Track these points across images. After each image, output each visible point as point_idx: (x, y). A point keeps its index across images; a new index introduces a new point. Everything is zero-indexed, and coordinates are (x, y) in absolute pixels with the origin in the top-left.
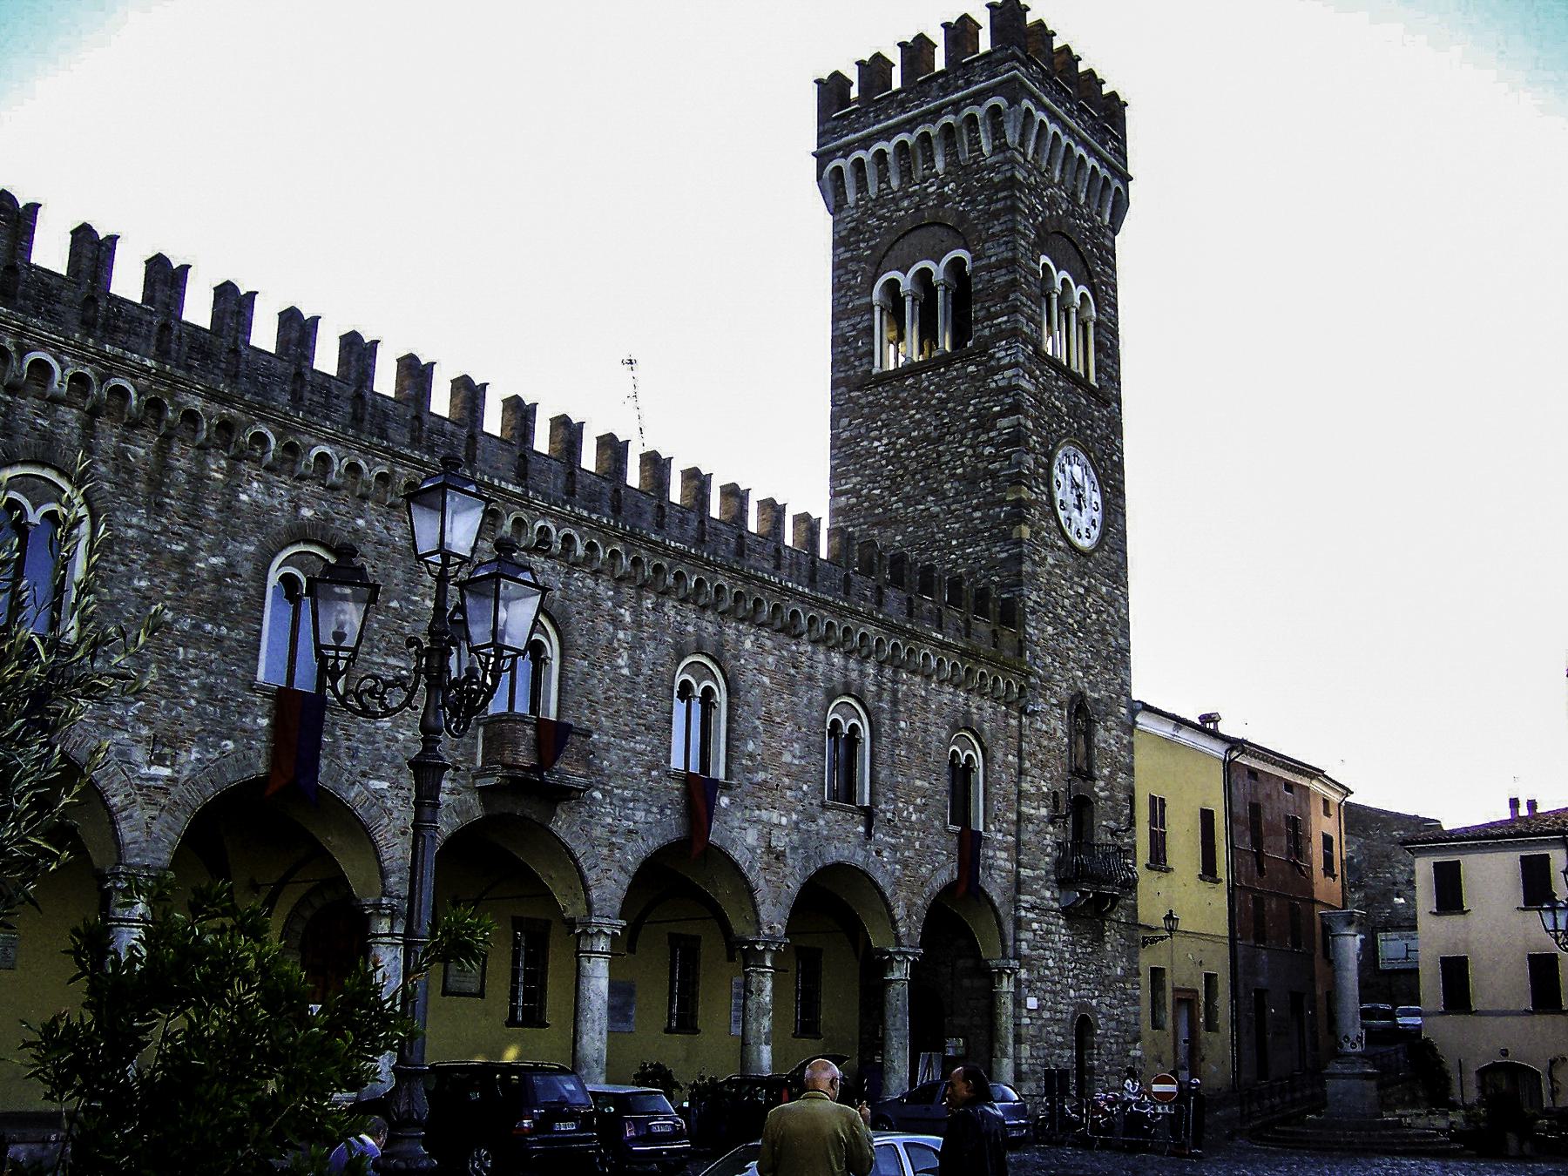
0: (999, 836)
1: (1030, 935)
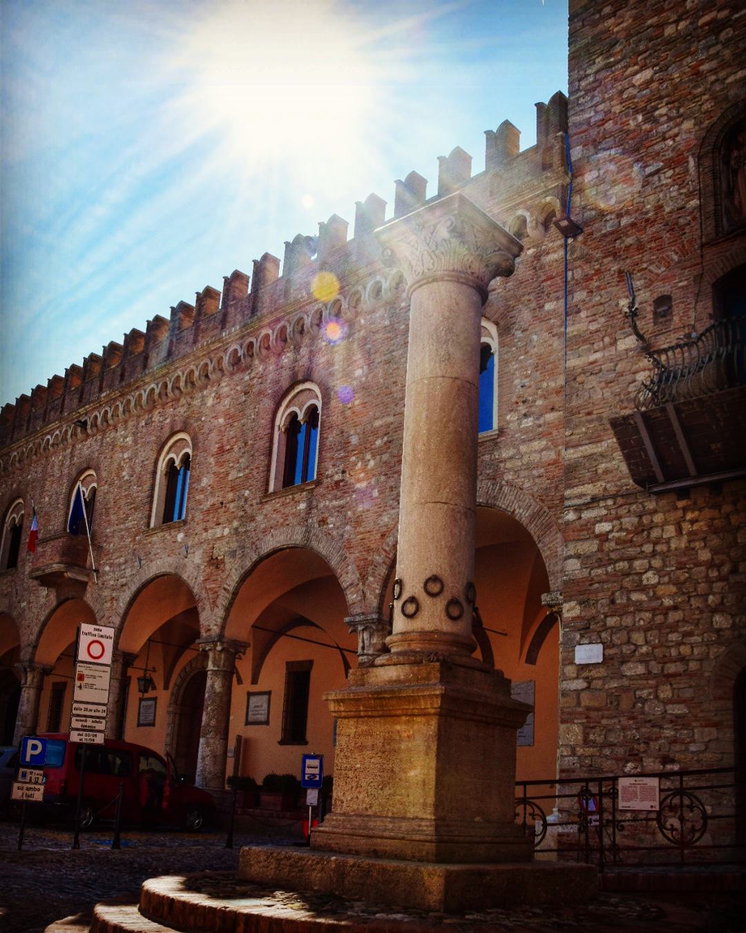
0: (528, 423)
1: (590, 547)
